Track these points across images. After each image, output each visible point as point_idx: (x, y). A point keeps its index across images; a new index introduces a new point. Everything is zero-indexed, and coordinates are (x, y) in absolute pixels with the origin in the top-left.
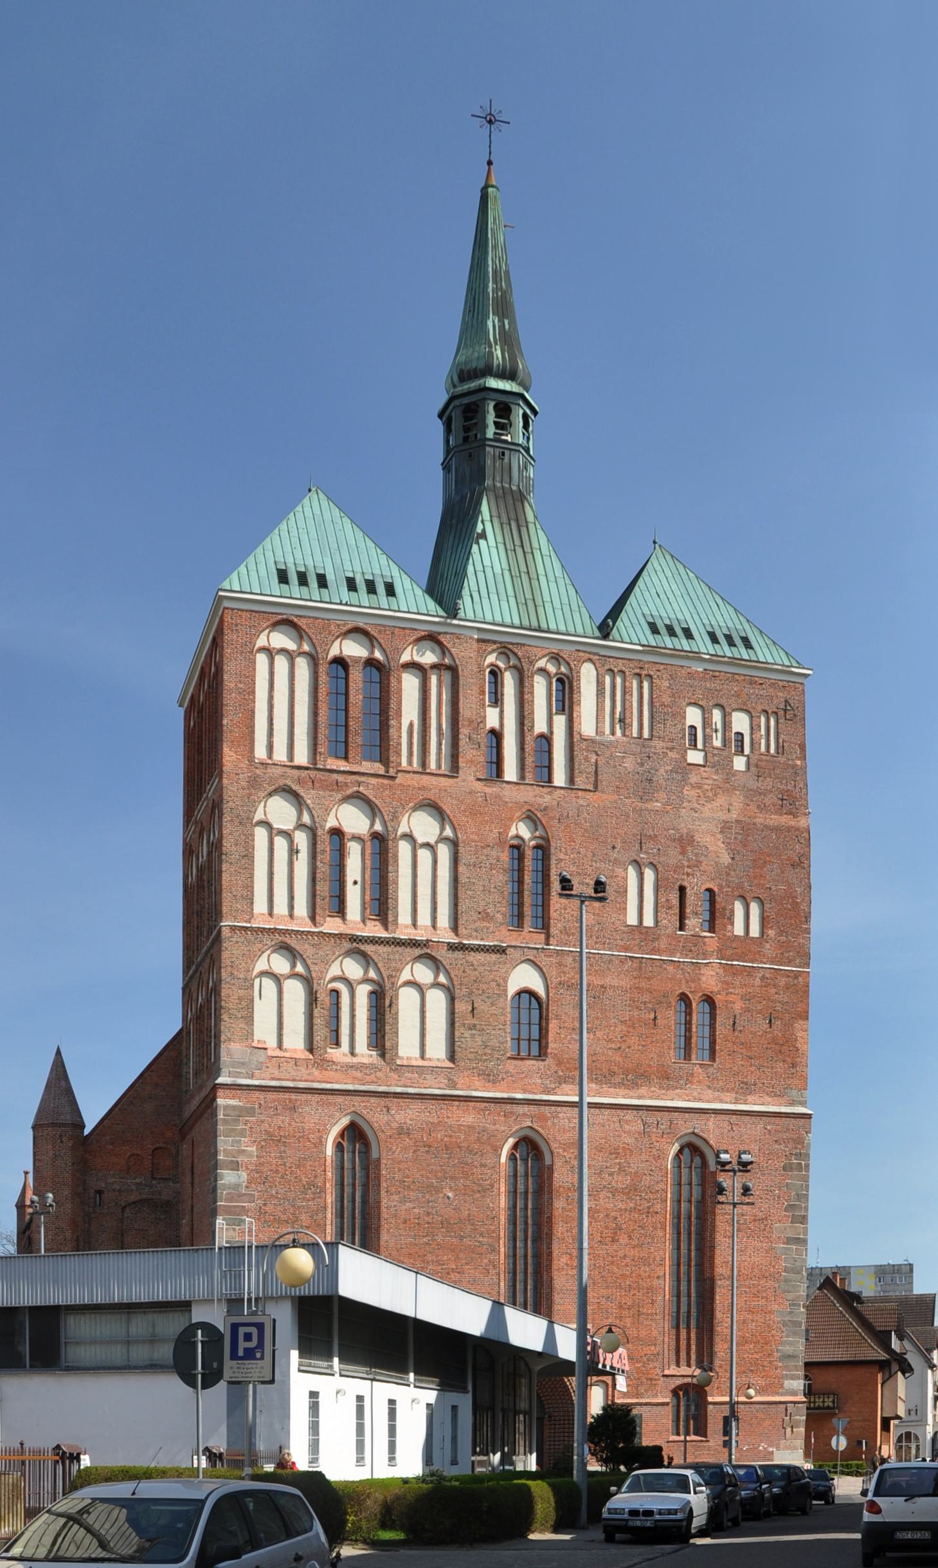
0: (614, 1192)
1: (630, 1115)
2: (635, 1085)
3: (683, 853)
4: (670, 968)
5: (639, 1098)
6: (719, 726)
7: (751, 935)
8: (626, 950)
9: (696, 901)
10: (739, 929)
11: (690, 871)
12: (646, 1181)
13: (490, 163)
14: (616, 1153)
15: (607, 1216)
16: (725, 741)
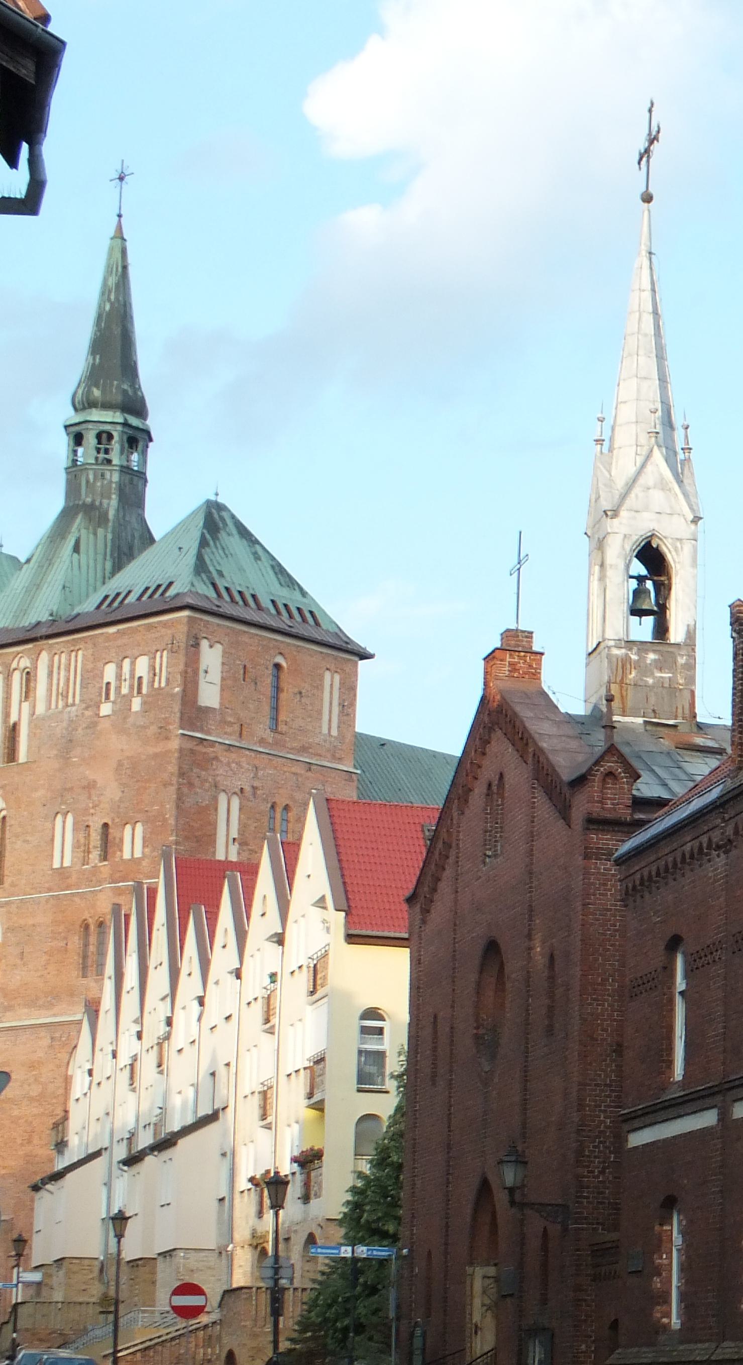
0: (31, 1099)
1: (43, 1033)
2: (51, 1005)
3: (90, 797)
4: (77, 899)
5: (54, 1015)
6: (128, 677)
7: (135, 856)
8: (50, 890)
9: (95, 838)
10: (127, 855)
11: (92, 811)
12: (51, 1087)
13: (120, 216)
14: (32, 1066)
15: (26, 1121)
16: (131, 687)
